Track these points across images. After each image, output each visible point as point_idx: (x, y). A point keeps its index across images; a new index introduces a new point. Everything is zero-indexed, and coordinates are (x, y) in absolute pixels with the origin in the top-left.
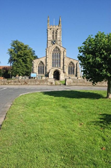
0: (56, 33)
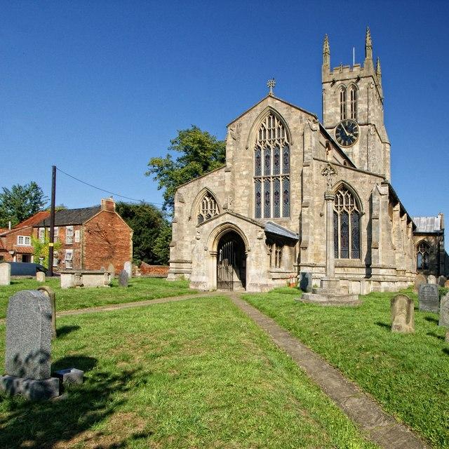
0: (354, 97)
